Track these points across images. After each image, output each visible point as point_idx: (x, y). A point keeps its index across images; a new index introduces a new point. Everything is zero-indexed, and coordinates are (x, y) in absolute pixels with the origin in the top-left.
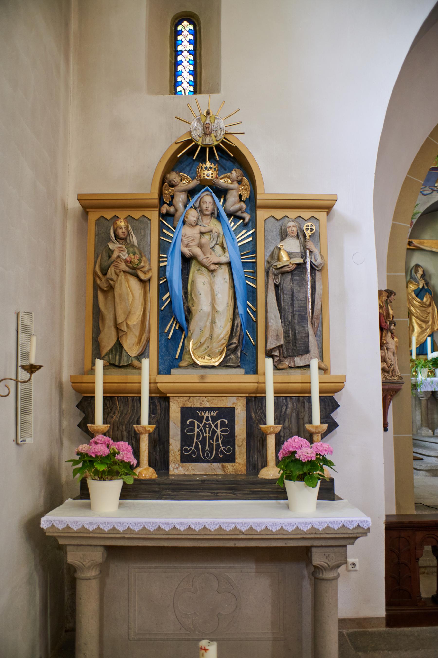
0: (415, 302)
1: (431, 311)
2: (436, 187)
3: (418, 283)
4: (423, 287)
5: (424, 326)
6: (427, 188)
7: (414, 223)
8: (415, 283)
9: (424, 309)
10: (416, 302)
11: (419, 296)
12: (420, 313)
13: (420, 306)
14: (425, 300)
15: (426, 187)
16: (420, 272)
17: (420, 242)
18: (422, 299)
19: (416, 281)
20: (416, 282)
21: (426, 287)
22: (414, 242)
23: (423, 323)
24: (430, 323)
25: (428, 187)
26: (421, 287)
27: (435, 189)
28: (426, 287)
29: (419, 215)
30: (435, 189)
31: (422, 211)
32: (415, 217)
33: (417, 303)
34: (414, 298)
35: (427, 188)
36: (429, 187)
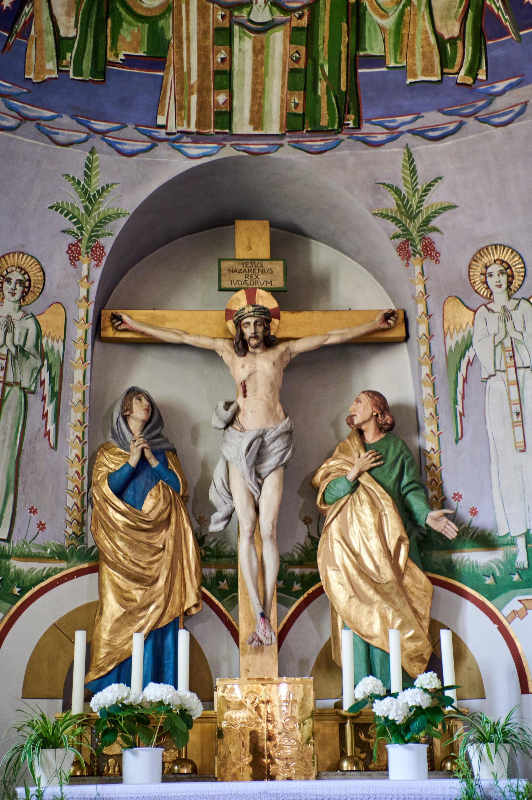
0: (111, 512)
1: (170, 543)
2: (164, 127)
3: (128, 450)
4: (143, 459)
5: (138, 594)
6: (130, 131)
7: (108, 250)
8: (119, 450)
9: (142, 536)
10: (117, 513)
11: (129, 493)
12: (126, 550)
13: (128, 525)
14: (148, 504)
15: (124, 126)
16: (139, 412)
17: (153, 317)
18: (137, 504)
19: (125, 445)
20: (121, 447)
21: (154, 463)
22: (125, 318)
23: (134, 585)
24: (161, 583)
25: (131, 127)
26: (133, 461)
27: (162, 133)
28: (154, 463)
29: (122, 222)
30: (162, 133)
31: (131, 212)
32: (107, 229)
33: (119, 517)
34: (106, 500)
35: (130, 131)
36: (136, 127)
